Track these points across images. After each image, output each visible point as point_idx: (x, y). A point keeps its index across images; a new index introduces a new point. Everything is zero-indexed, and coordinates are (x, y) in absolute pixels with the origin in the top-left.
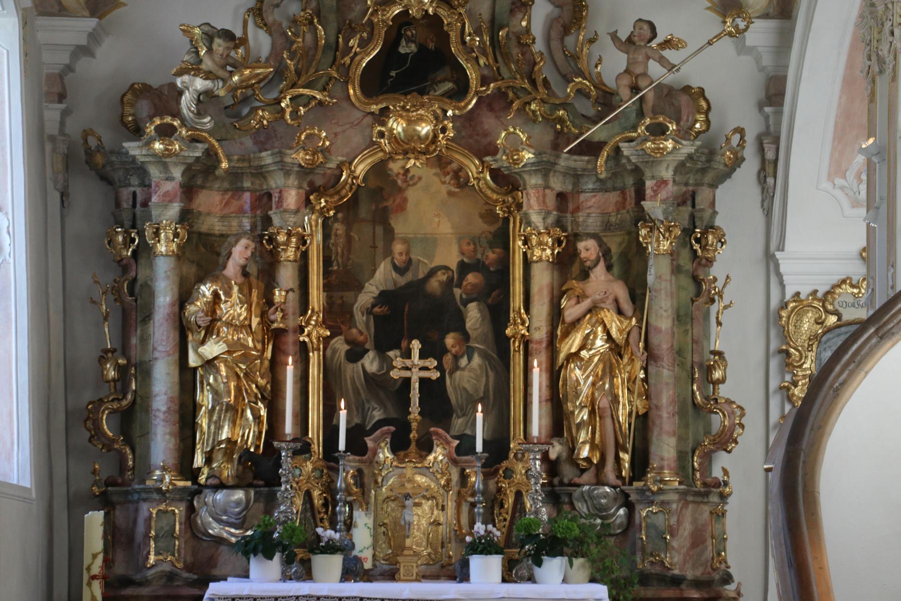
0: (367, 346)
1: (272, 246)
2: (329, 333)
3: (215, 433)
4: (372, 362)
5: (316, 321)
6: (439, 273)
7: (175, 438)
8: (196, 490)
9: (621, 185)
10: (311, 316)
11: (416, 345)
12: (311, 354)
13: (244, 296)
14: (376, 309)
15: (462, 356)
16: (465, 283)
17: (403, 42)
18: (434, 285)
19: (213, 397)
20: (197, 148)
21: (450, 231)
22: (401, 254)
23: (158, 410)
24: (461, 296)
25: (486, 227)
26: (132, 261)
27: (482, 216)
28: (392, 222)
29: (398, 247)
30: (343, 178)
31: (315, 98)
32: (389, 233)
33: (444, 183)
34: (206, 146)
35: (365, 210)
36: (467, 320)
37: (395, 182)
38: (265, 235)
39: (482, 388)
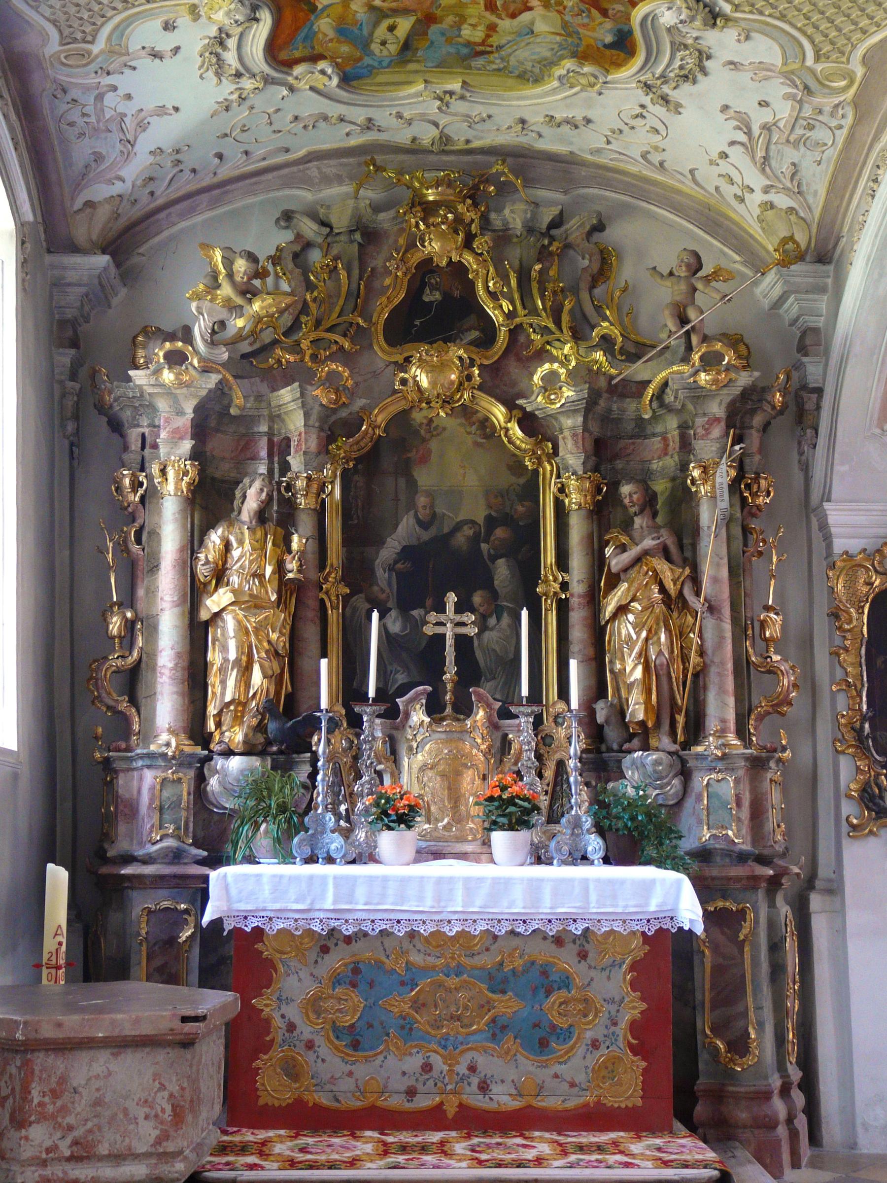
0: (390, 605)
2: (348, 591)
4: (394, 622)
5: (335, 578)
6: (466, 527)
7: (184, 699)
8: (206, 756)
9: (663, 430)
10: (329, 573)
11: (451, 598)
14: (399, 566)
15: (490, 616)
16: (492, 538)
17: (427, 290)
18: (461, 540)
20: (210, 378)
21: (477, 483)
22: (425, 507)
24: (489, 551)
25: (513, 479)
26: (140, 506)
27: (510, 468)
28: (415, 474)
29: (422, 500)
30: (364, 427)
31: (336, 342)
32: (412, 484)
33: (469, 433)
34: (220, 377)
35: (388, 461)
36: (496, 577)
37: (417, 432)
38: (283, 481)
39: (513, 649)
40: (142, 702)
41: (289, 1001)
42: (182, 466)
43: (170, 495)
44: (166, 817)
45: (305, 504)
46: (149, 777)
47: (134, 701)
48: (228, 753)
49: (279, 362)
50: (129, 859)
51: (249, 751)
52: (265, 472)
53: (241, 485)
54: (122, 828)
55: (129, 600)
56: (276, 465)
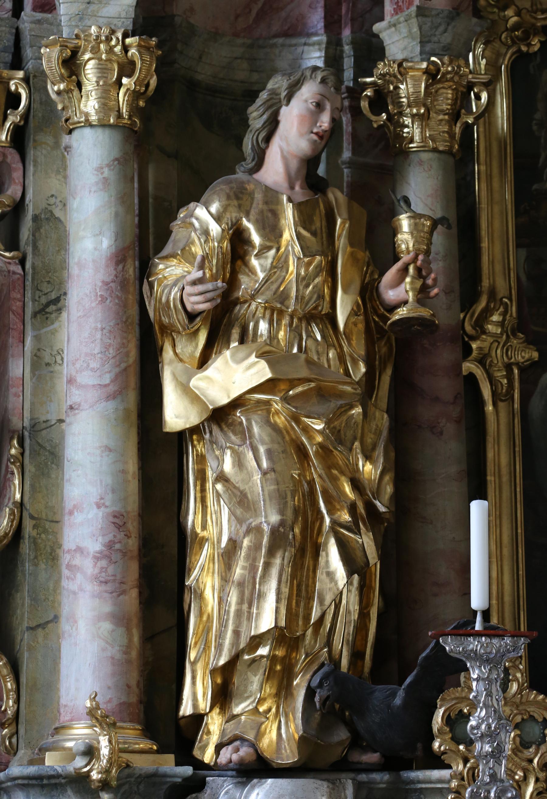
1: (384, 116)
2: (536, 355)
3: (239, 614)
5: (502, 324)
7: (129, 630)
8: (187, 780)
10: (487, 312)
12: (490, 408)
13: (314, 234)
19: (232, 513)
23: (79, 550)
26: (13, 156)
42: (118, 49)
43: (88, 124)
45: (424, 139)
52: (320, 63)
53: (264, 96)
56: (347, 49)
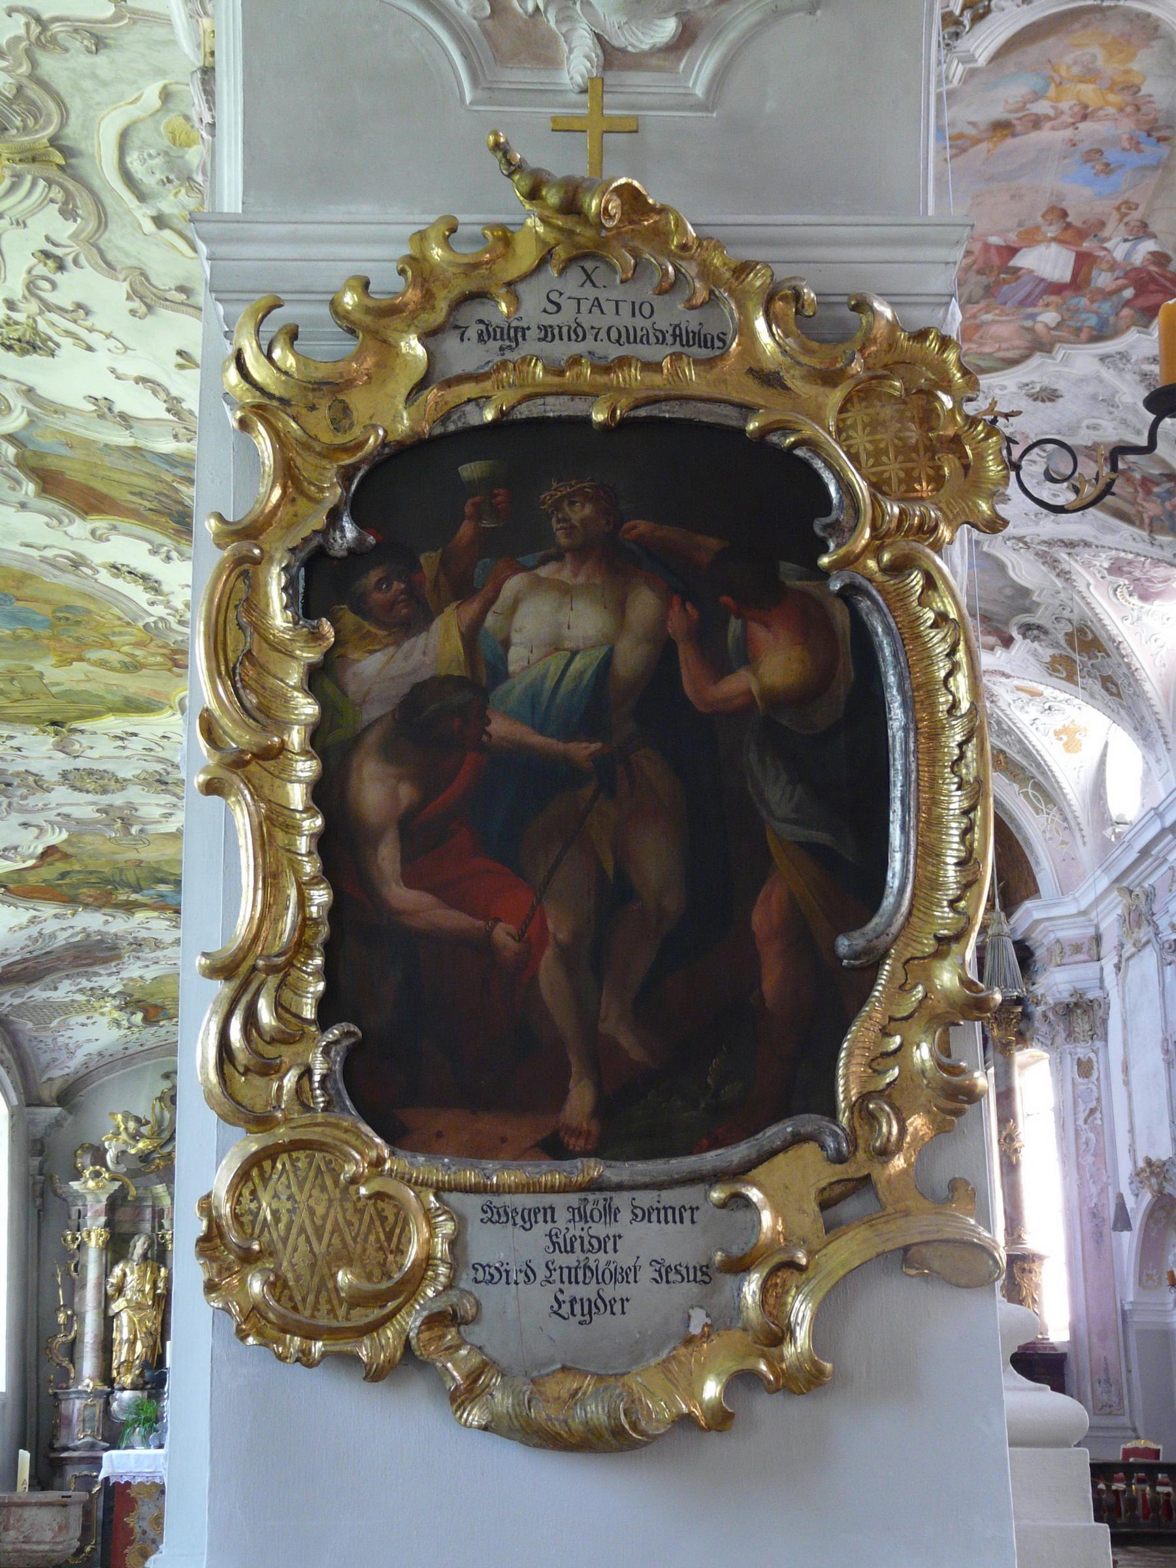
40: (76, 1361)
41: (143, 1519)
44: (87, 1425)
46: (78, 1404)
47: (72, 1361)
48: (123, 1389)
49: (158, 1167)
50: (66, 1449)
51: (134, 1387)
54: (63, 1432)
55: (69, 1304)
